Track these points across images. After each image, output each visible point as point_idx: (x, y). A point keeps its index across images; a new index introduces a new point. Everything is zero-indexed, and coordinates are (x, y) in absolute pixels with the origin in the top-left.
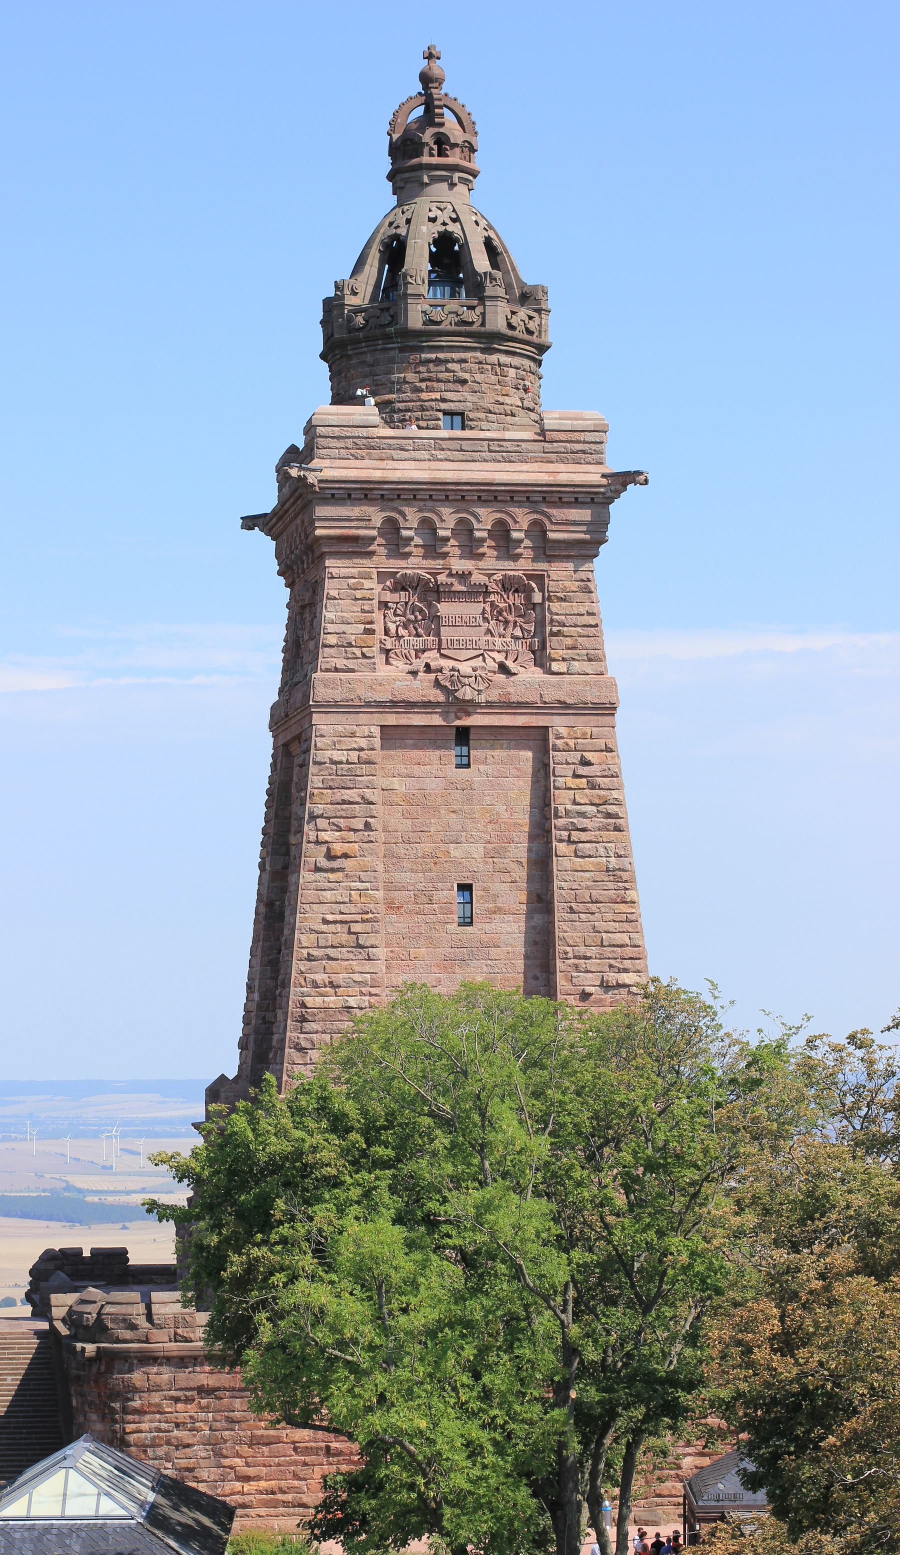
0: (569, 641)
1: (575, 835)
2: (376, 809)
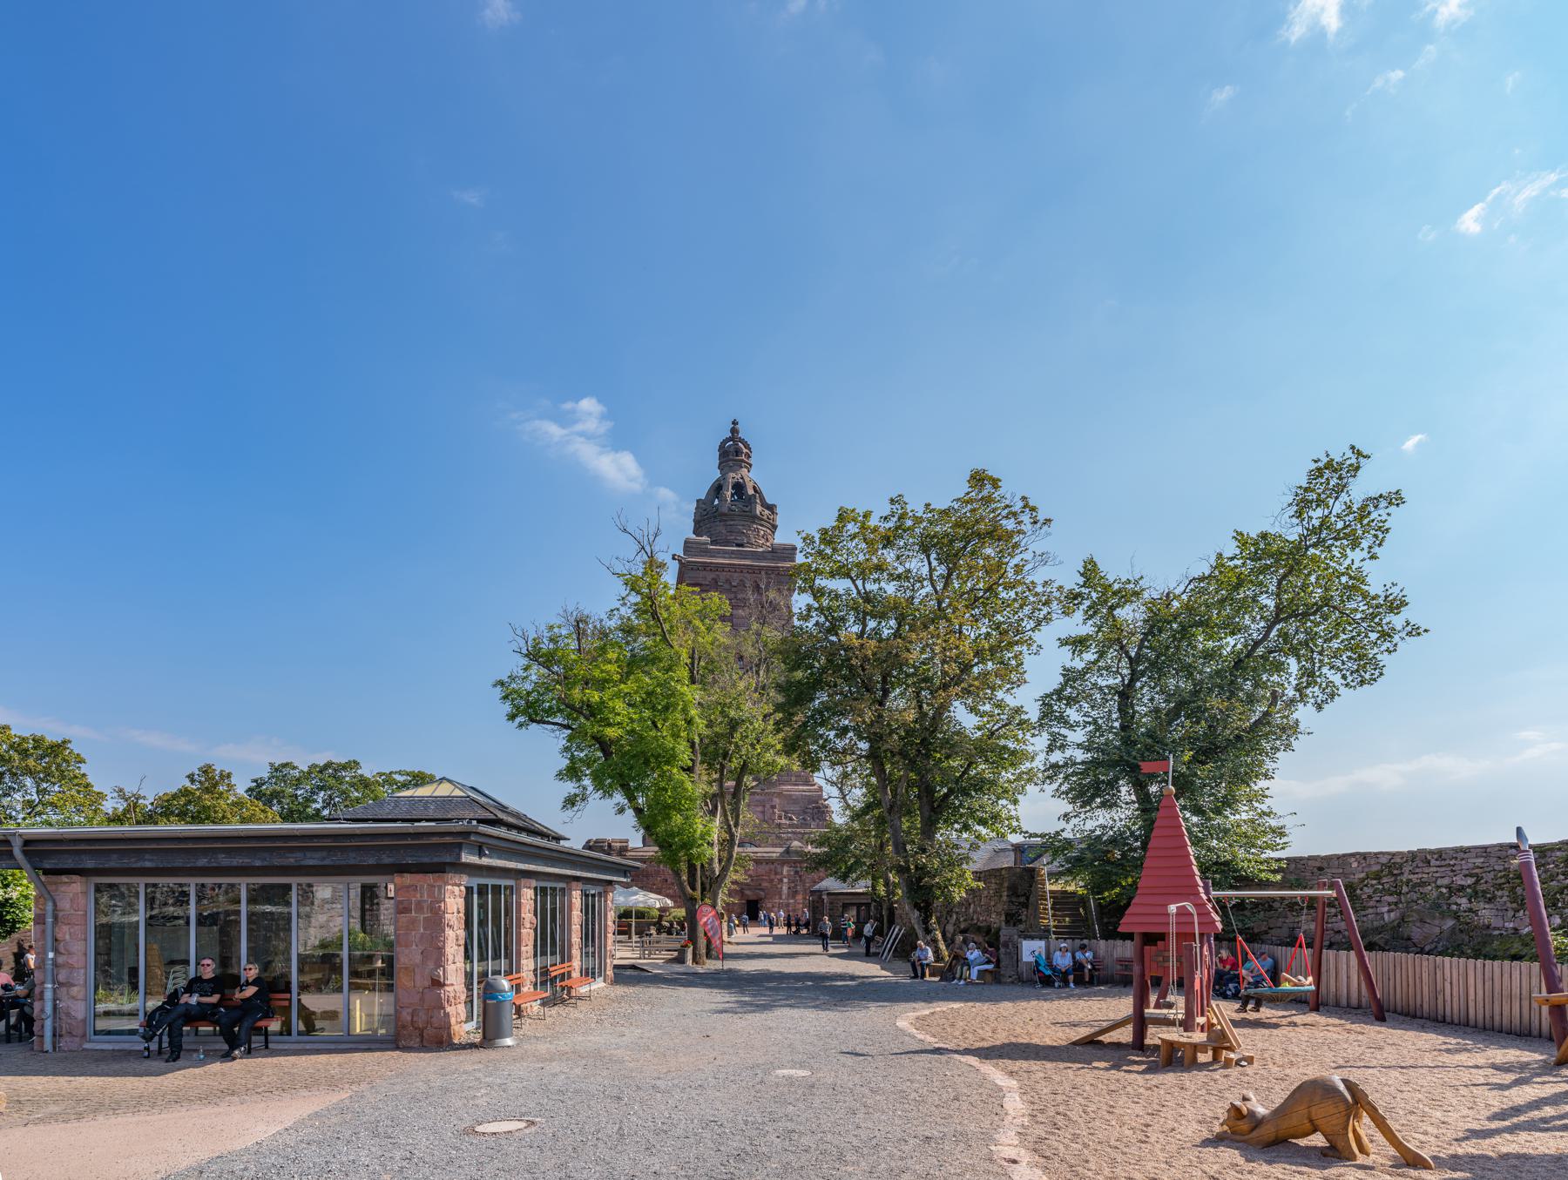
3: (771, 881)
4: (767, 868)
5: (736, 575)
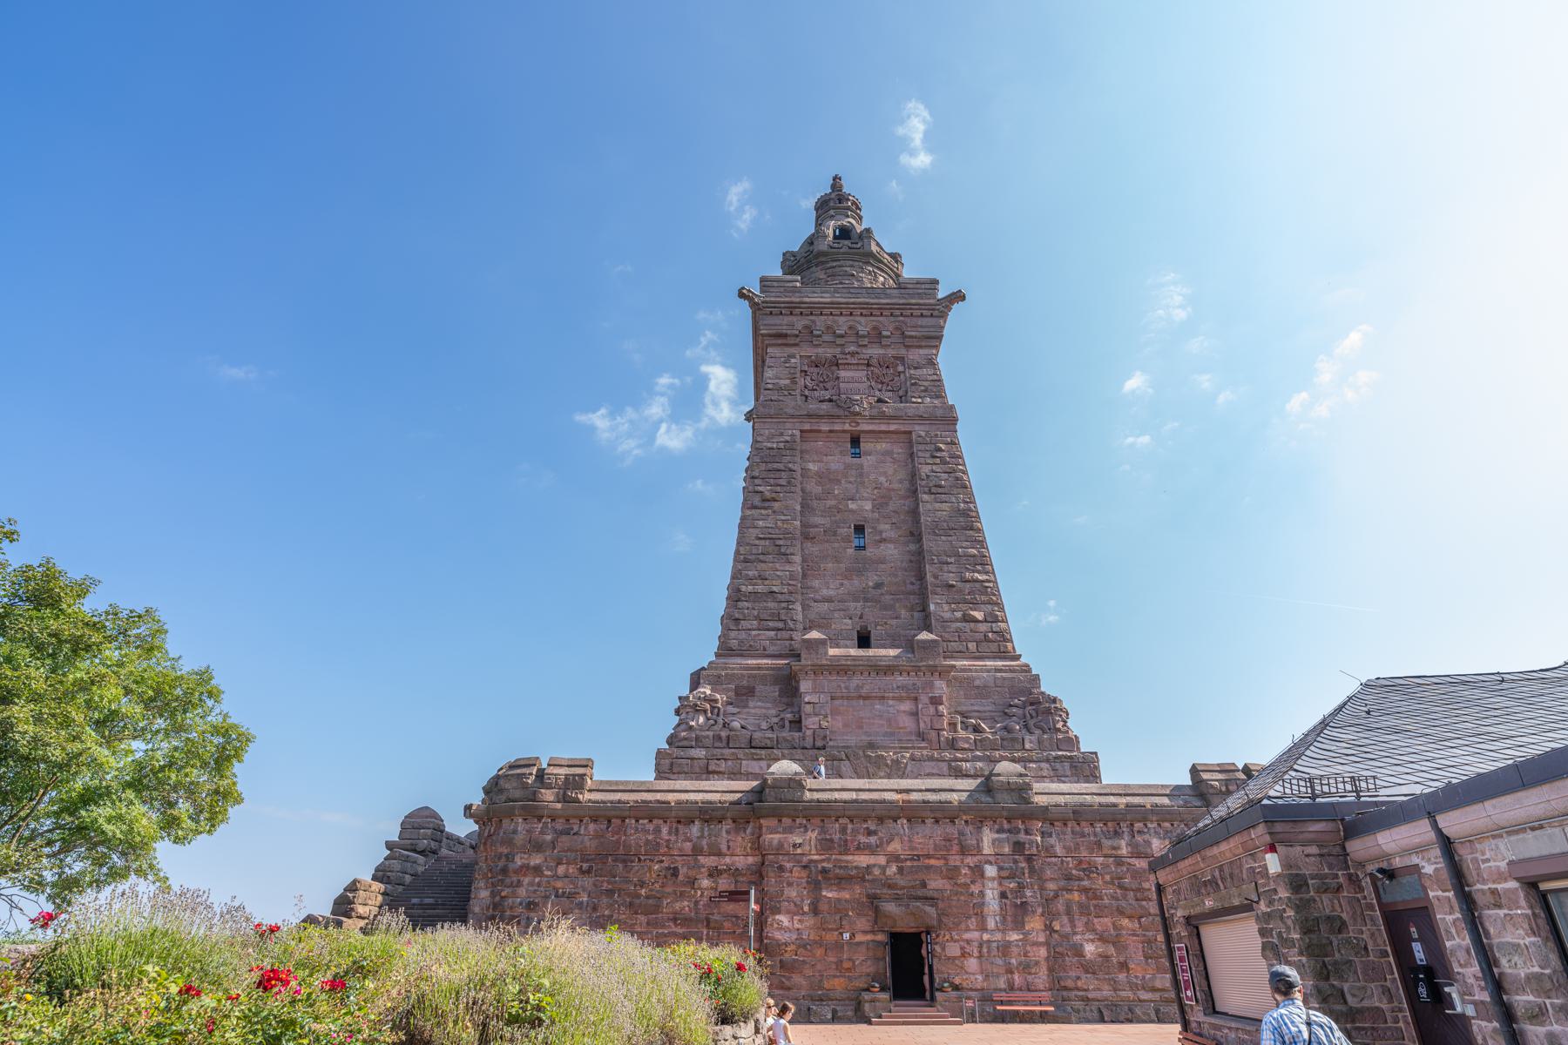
0: (923, 388)
2: (798, 475)
3: (952, 873)
5: (842, 319)
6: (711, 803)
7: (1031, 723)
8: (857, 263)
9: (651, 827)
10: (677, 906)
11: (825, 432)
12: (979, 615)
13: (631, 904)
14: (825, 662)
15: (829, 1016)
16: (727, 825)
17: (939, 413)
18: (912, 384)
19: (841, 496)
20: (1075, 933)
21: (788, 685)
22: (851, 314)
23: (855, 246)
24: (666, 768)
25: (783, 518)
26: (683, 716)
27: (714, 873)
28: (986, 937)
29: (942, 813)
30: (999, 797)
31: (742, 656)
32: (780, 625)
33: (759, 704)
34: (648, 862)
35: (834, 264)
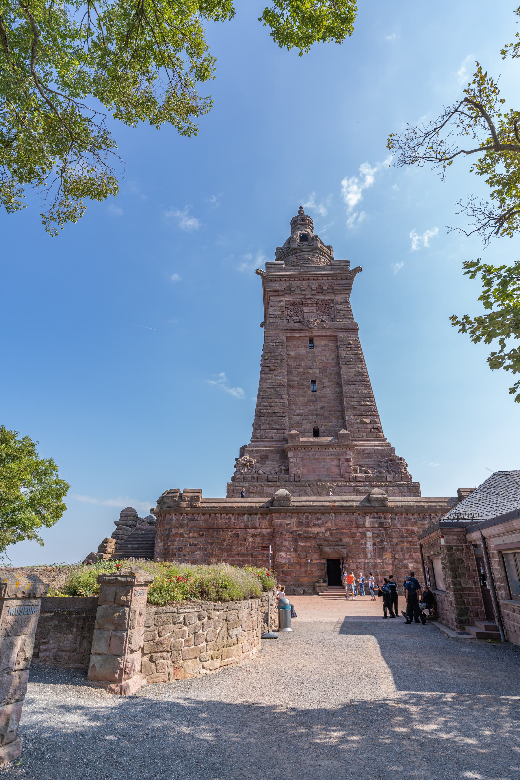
1: (347, 363)
3: (353, 535)
4: (347, 518)
5: (304, 282)
6: (251, 507)
7: (390, 469)
8: (311, 253)
9: (227, 517)
10: (239, 549)
11: (297, 337)
12: (368, 421)
13: (220, 548)
14: (298, 444)
15: (302, 592)
16: (258, 516)
17: (350, 326)
18: (338, 313)
19: (305, 367)
20: (405, 559)
21: (283, 455)
22: (308, 279)
23: (310, 244)
24: (231, 491)
25: (279, 378)
26: (238, 468)
27: (254, 536)
28: (367, 561)
29: (349, 511)
30: (373, 503)
31: (262, 441)
32: (279, 427)
33: (270, 462)
34: (226, 532)
35: (300, 254)
